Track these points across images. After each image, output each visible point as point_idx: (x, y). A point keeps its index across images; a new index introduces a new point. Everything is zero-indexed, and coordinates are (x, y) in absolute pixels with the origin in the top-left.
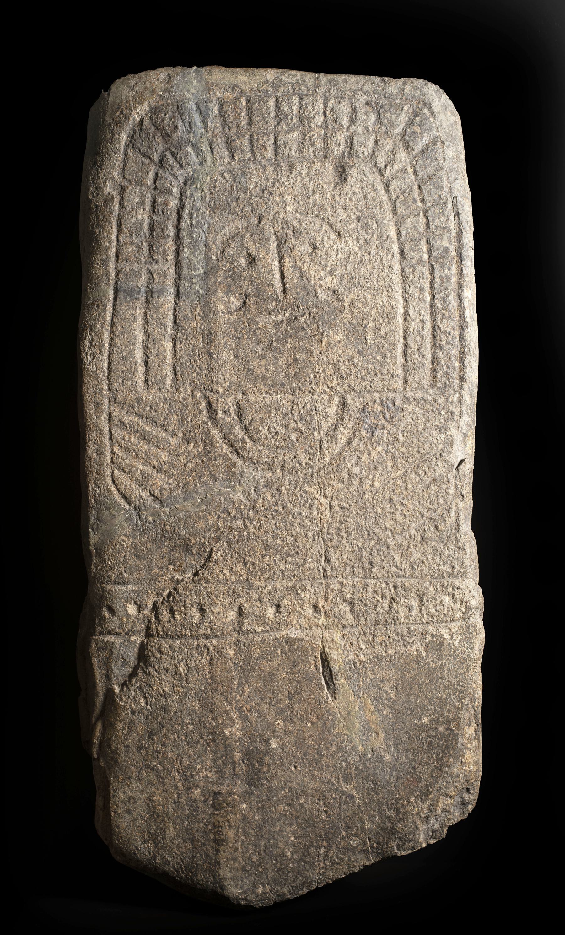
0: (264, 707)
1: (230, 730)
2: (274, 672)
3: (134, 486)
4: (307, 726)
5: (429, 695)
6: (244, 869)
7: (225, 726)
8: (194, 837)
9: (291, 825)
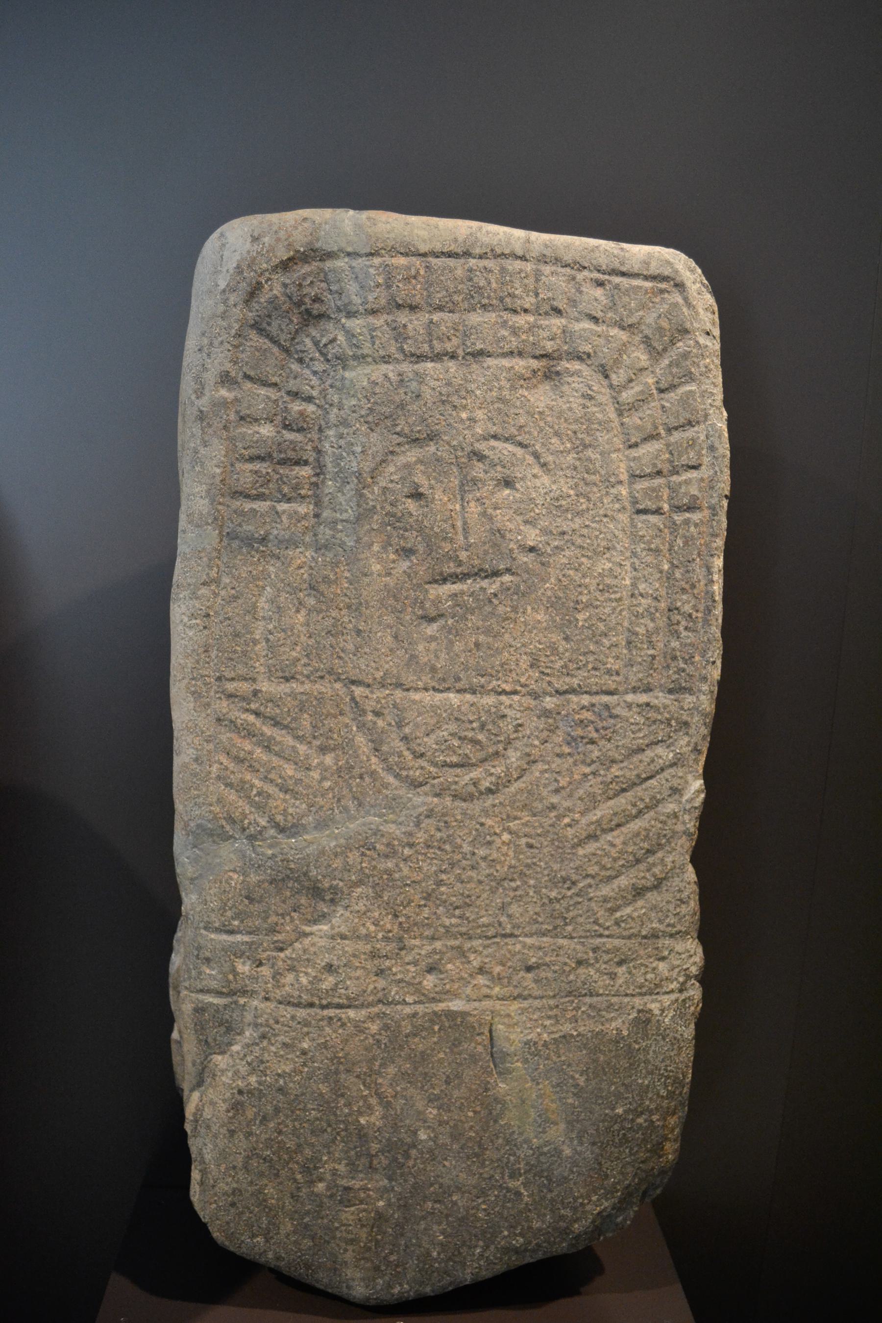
0: (412, 1091)
1: (367, 1118)
2: (429, 1052)
4: (466, 1117)
7: (360, 1113)
9: (440, 1224)
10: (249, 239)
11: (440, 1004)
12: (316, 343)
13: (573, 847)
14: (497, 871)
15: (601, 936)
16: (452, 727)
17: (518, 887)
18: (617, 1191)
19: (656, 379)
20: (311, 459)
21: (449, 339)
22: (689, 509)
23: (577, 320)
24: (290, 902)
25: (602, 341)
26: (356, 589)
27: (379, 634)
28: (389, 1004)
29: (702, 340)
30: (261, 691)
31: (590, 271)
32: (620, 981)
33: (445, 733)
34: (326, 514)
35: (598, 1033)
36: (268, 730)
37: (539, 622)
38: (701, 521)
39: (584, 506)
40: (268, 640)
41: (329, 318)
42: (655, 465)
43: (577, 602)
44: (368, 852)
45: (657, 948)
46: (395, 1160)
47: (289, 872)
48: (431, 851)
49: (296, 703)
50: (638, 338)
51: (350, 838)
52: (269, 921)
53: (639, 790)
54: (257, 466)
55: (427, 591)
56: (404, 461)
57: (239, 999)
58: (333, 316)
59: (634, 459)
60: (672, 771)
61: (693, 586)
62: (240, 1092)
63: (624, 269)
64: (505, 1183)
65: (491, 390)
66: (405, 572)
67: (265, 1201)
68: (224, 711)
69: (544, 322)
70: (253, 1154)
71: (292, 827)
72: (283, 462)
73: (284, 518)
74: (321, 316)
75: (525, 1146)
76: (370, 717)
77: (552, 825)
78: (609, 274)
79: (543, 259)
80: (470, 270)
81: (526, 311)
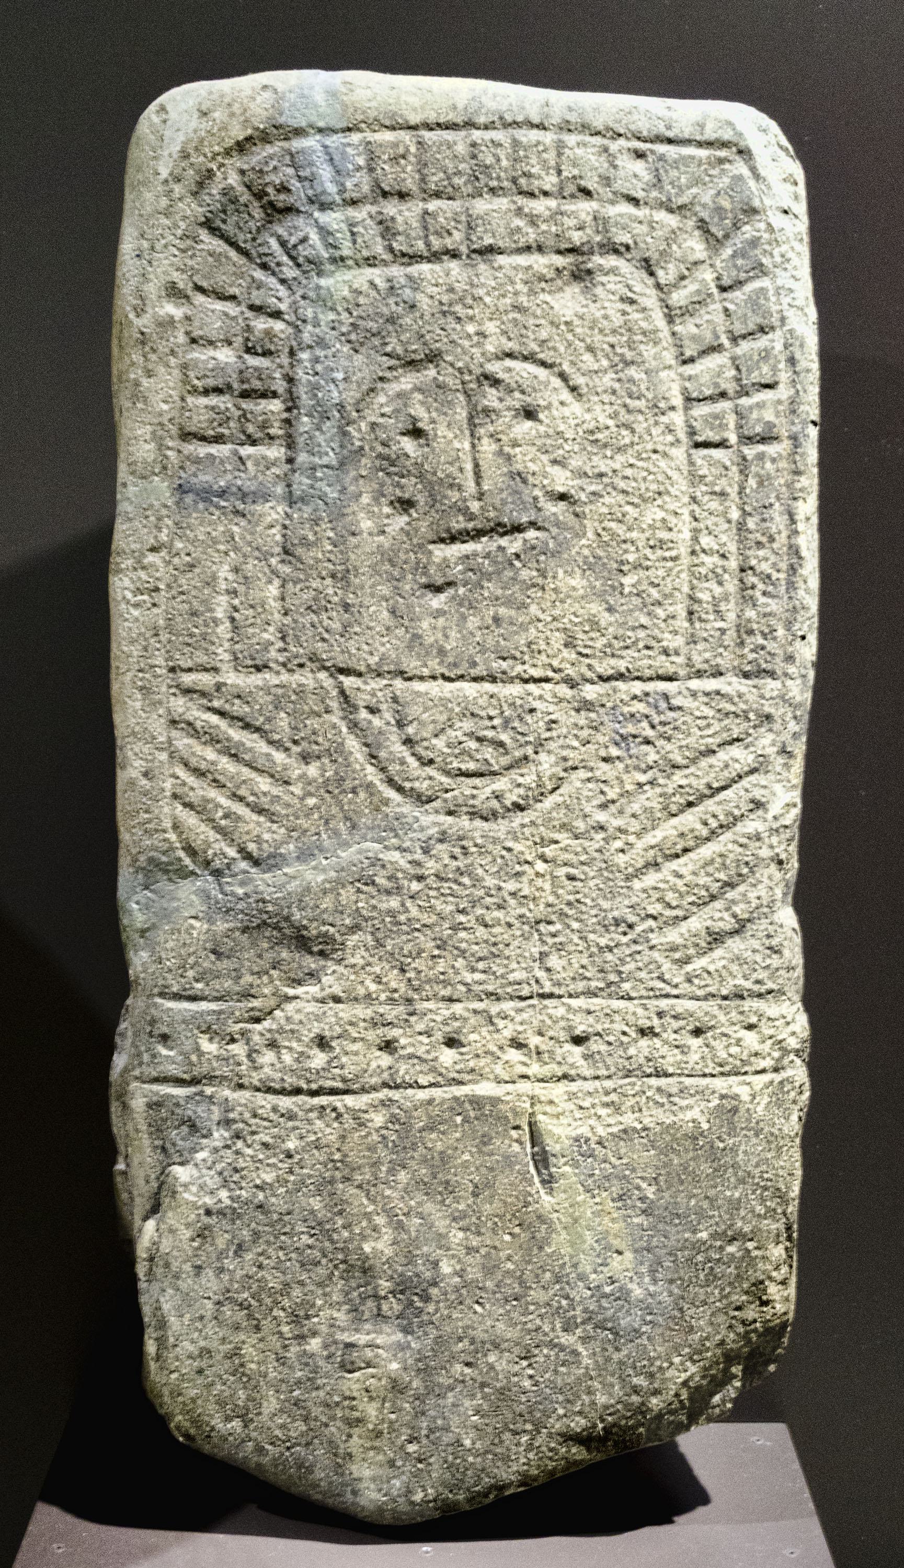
0: (429, 1207)
1: (373, 1244)
2: (450, 1152)
3: (212, 835)
5: (712, 1193)
6: (392, 1463)
7: (364, 1238)
8: (309, 1413)
10: (196, 115)
11: (463, 1087)
12: (283, 243)
13: (628, 878)
14: (530, 910)
15: (667, 996)
16: (468, 725)
17: (559, 931)
18: (708, 1349)
19: (715, 275)
20: (281, 391)
21: (450, 234)
22: (764, 439)
23: (613, 203)
24: (269, 956)
25: (644, 228)
26: (341, 552)
27: (372, 609)
28: (397, 1087)
29: (777, 220)
30: (225, 684)
31: (627, 139)
32: (694, 1057)
33: (459, 733)
34: (302, 458)
35: (669, 1126)
36: (236, 734)
37: (574, 589)
38: (780, 455)
39: (627, 441)
40: (233, 620)
41: (298, 211)
42: (716, 385)
43: (622, 563)
44: (365, 888)
45: (742, 1013)
46: (411, 1303)
47: (265, 916)
48: (446, 885)
49: (269, 698)
50: (691, 223)
51: (343, 870)
52: (242, 981)
53: (710, 805)
54: (213, 400)
55: (430, 552)
56: (398, 389)
57: (205, 1088)
58: (302, 209)
59: (690, 378)
60: (753, 778)
61: (772, 539)
62: (208, 1213)
63: (670, 134)
64: (558, 1337)
65: (504, 296)
66: (402, 529)
67: (242, 1365)
68: (181, 710)
69: (568, 207)
70: (226, 1298)
71: (269, 857)
72: (245, 395)
73: (249, 464)
74: (289, 210)
75: (580, 1284)
76: (364, 714)
77: (599, 851)
78: (652, 142)
79: (566, 127)
80: (474, 145)
81: (546, 194)
